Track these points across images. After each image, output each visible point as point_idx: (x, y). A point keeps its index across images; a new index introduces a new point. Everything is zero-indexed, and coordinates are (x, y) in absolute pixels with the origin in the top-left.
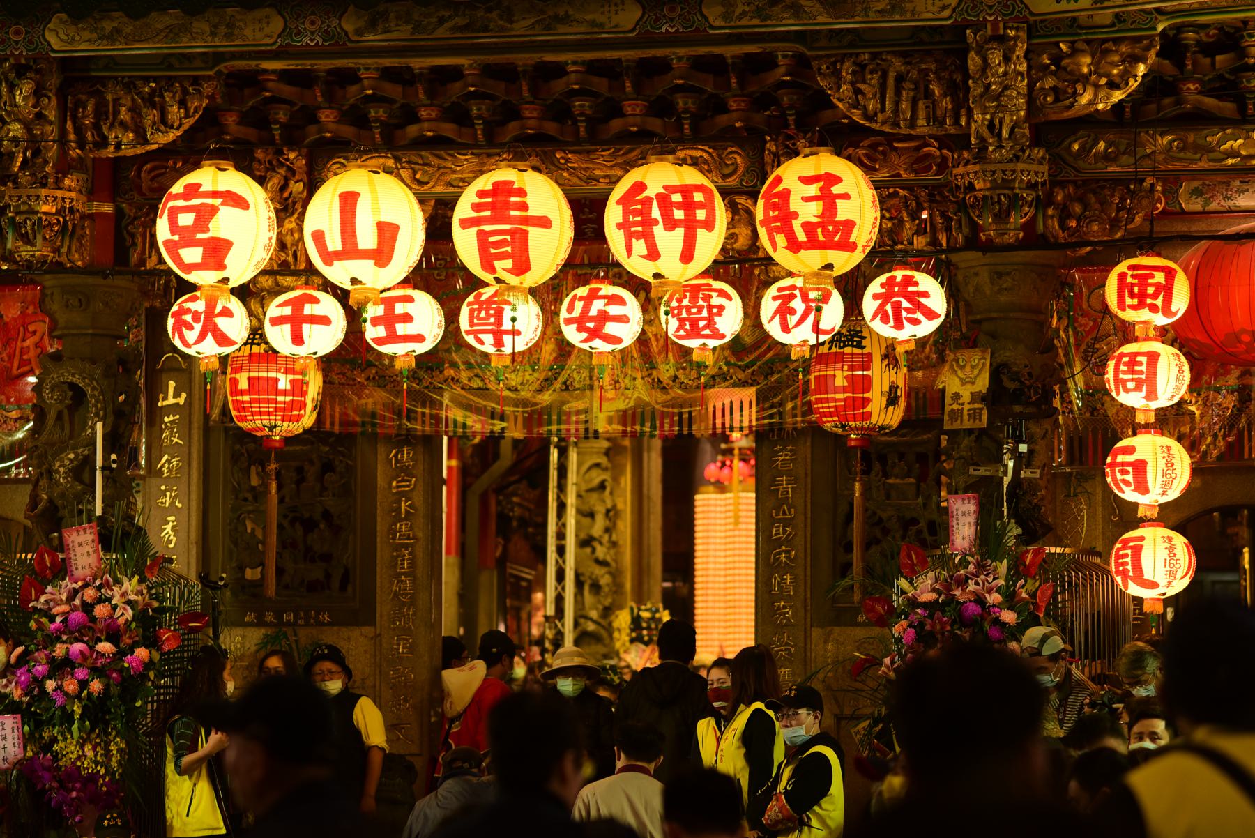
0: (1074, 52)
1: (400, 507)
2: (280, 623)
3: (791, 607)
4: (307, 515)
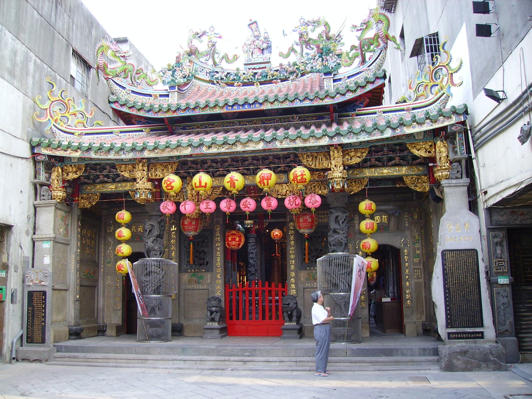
0: (351, 152)
2: (195, 272)
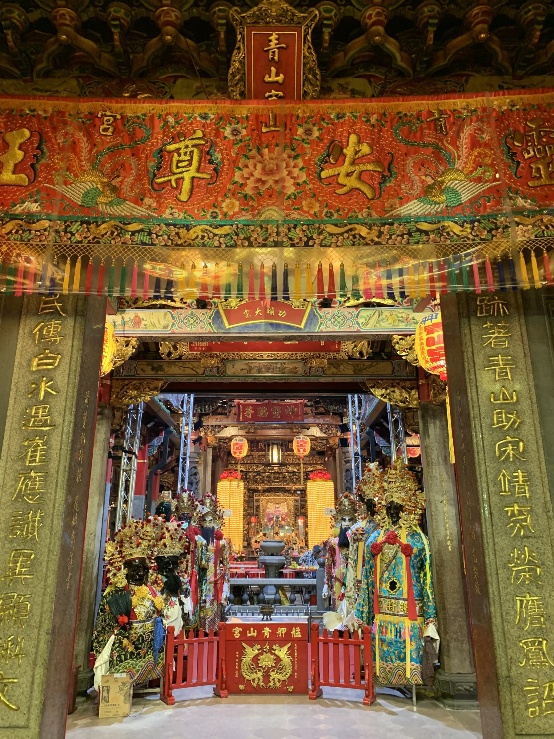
1: (38, 389)
3: (529, 512)
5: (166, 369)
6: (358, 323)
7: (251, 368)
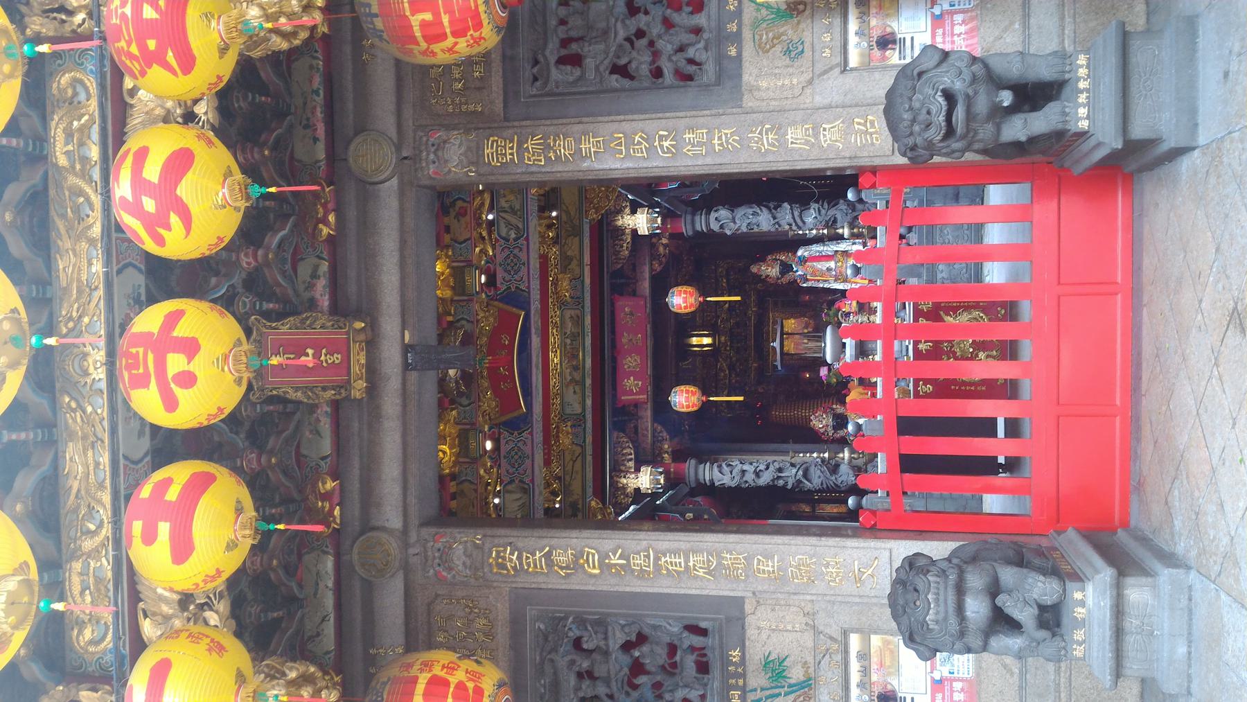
3: (720, 132)
4: (626, 670)
5: (575, 497)
6: (516, 240)
7: (573, 381)
